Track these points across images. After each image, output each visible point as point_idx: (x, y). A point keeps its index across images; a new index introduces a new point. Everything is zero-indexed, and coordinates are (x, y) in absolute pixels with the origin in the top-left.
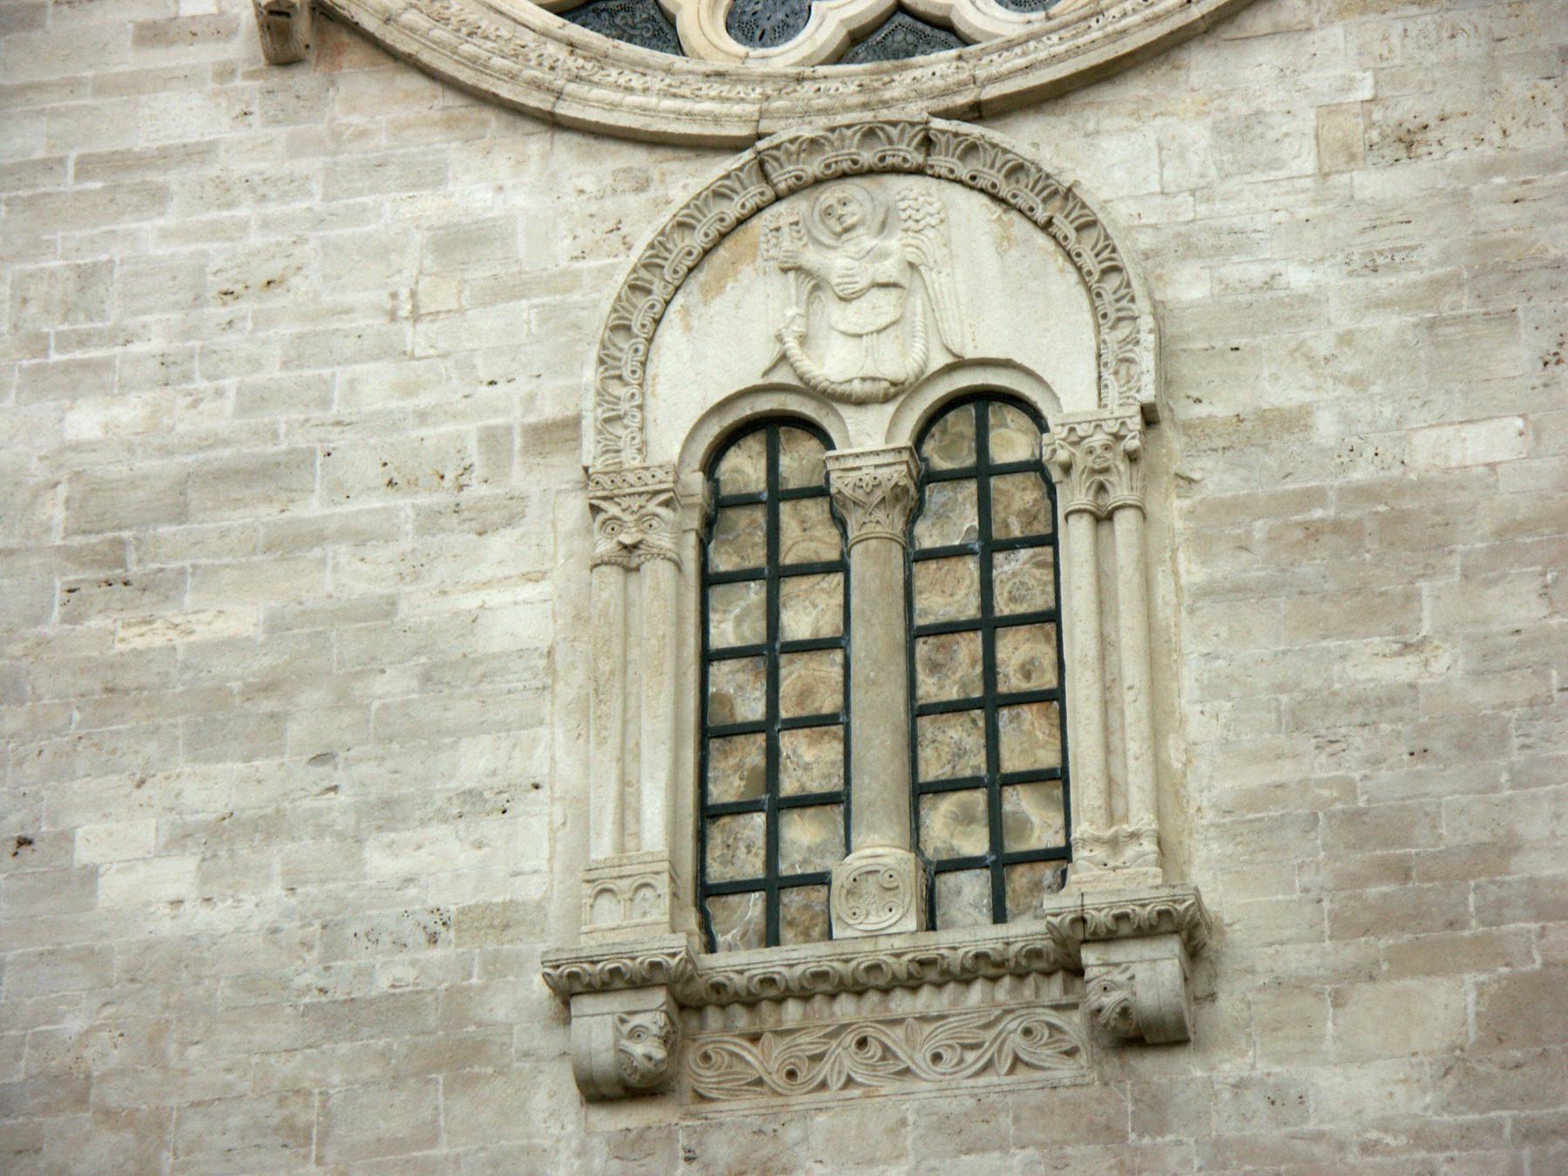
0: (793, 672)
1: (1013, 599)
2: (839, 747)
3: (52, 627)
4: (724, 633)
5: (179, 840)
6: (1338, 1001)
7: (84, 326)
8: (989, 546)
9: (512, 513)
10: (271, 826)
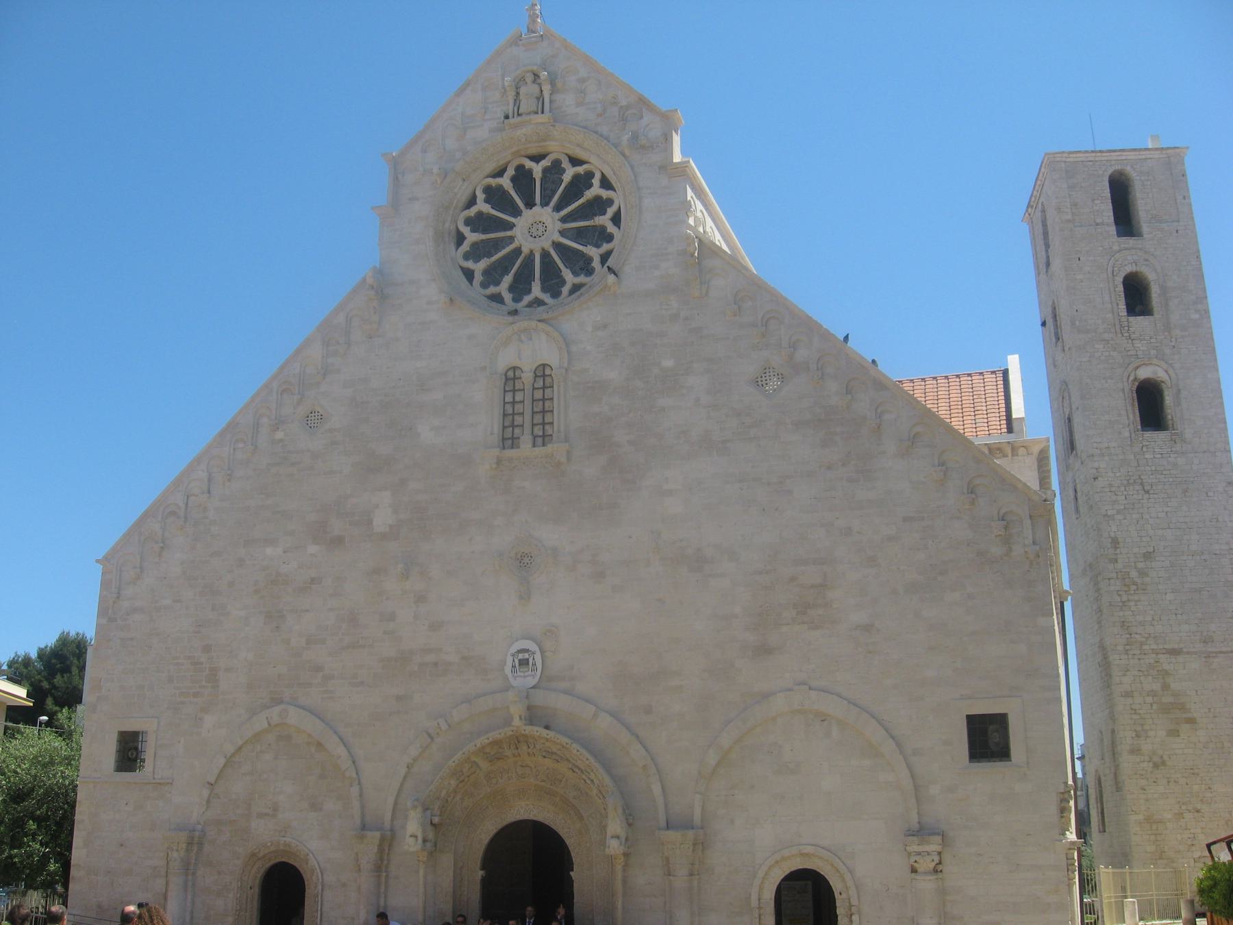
2: (522, 419)
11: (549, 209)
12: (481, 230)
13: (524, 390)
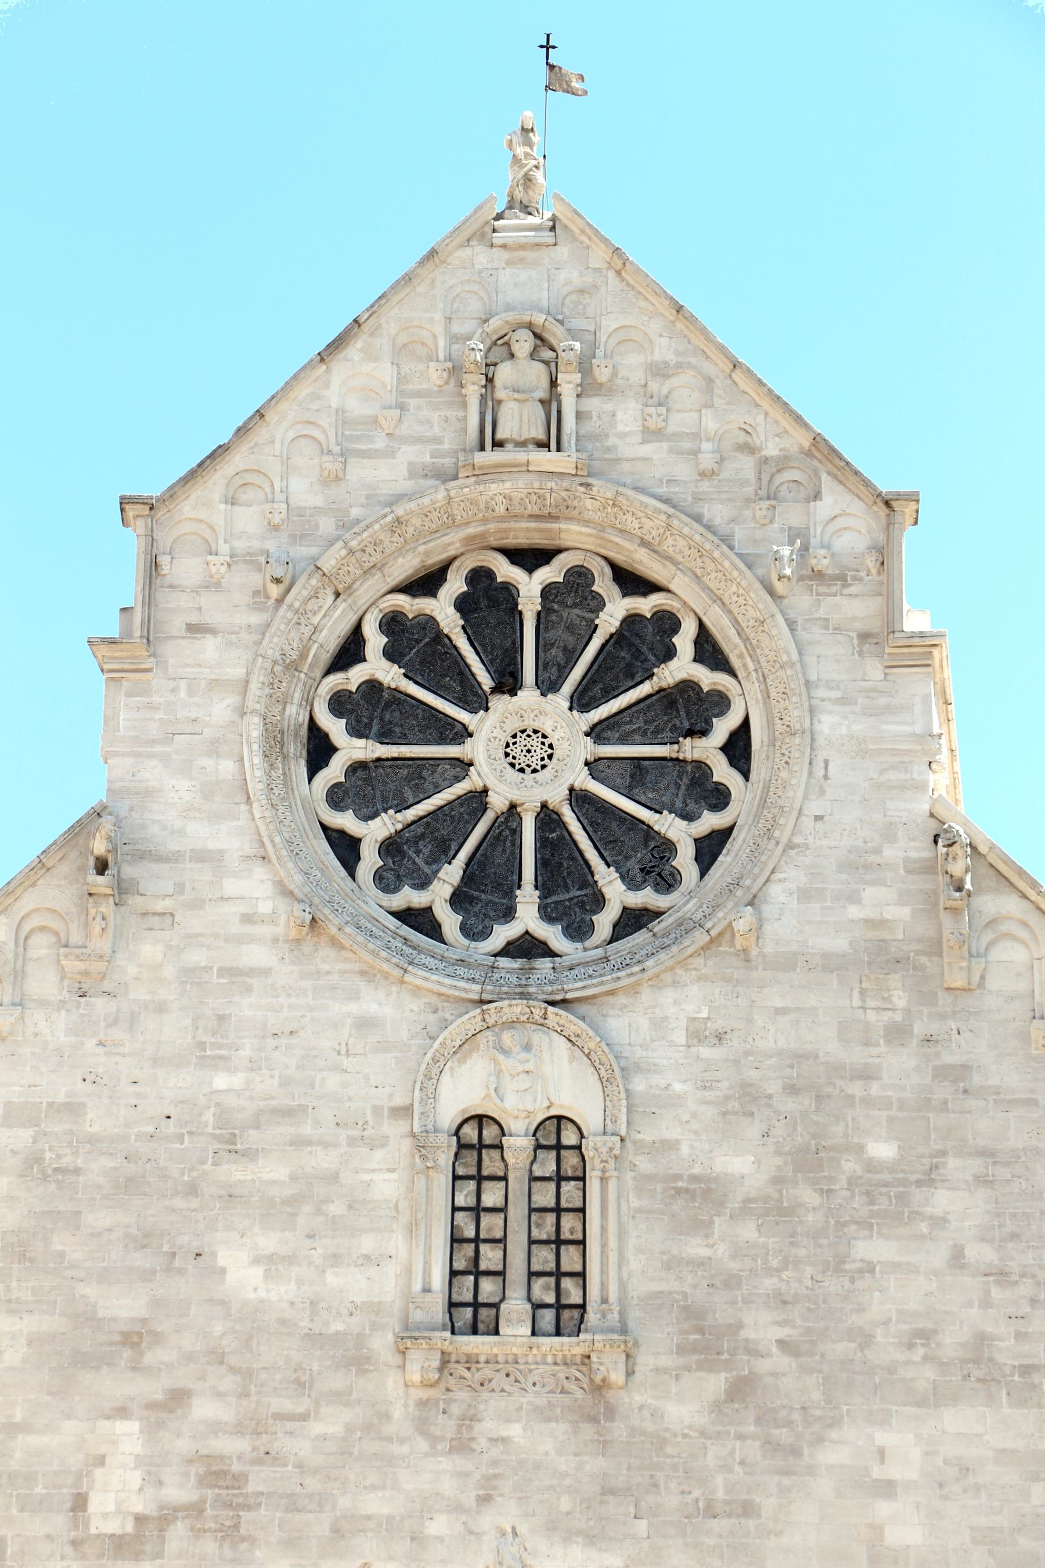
0: (486, 1220)
1: (567, 1201)
2: (502, 1253)
3: (208, 1167)
4: (461, 1201)
5: (257, 1261)
6: (677, 1377)
7: (220, 1040)
8: (560, 1178)
9: (383, 1142)
10: (291, 1259)
11: (560, 700)
12: (375, 727)
13: (504, 1178)
